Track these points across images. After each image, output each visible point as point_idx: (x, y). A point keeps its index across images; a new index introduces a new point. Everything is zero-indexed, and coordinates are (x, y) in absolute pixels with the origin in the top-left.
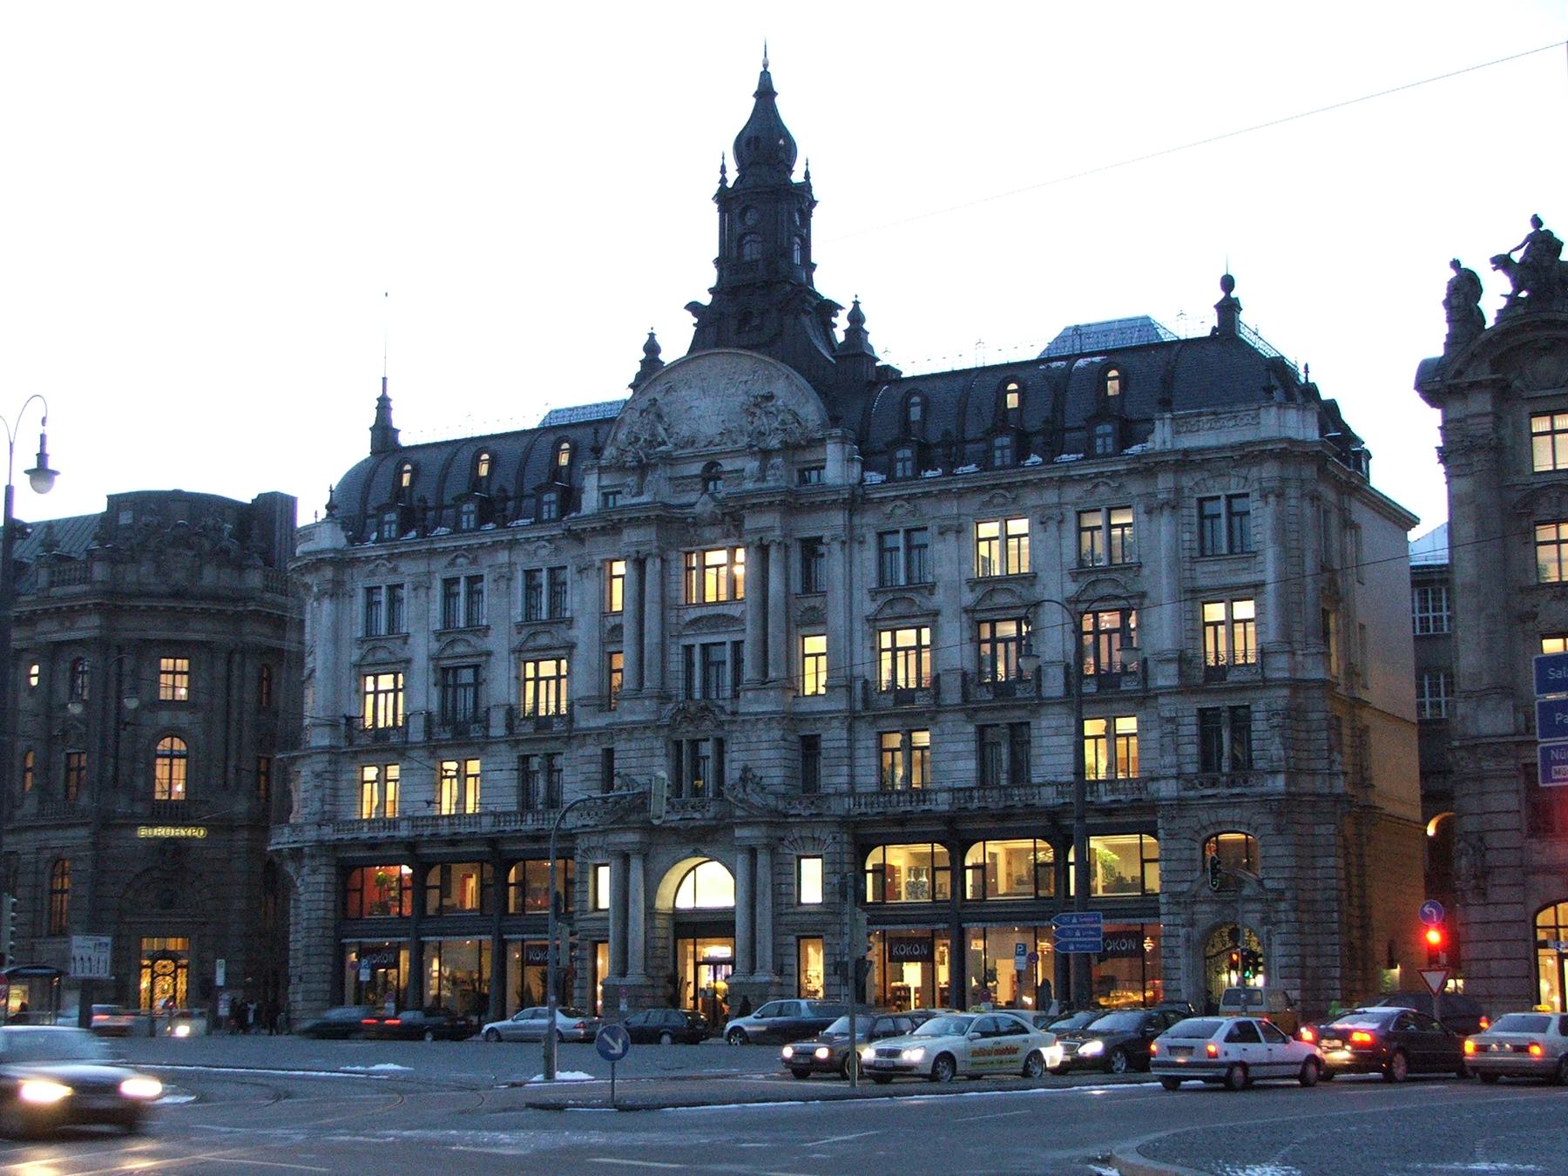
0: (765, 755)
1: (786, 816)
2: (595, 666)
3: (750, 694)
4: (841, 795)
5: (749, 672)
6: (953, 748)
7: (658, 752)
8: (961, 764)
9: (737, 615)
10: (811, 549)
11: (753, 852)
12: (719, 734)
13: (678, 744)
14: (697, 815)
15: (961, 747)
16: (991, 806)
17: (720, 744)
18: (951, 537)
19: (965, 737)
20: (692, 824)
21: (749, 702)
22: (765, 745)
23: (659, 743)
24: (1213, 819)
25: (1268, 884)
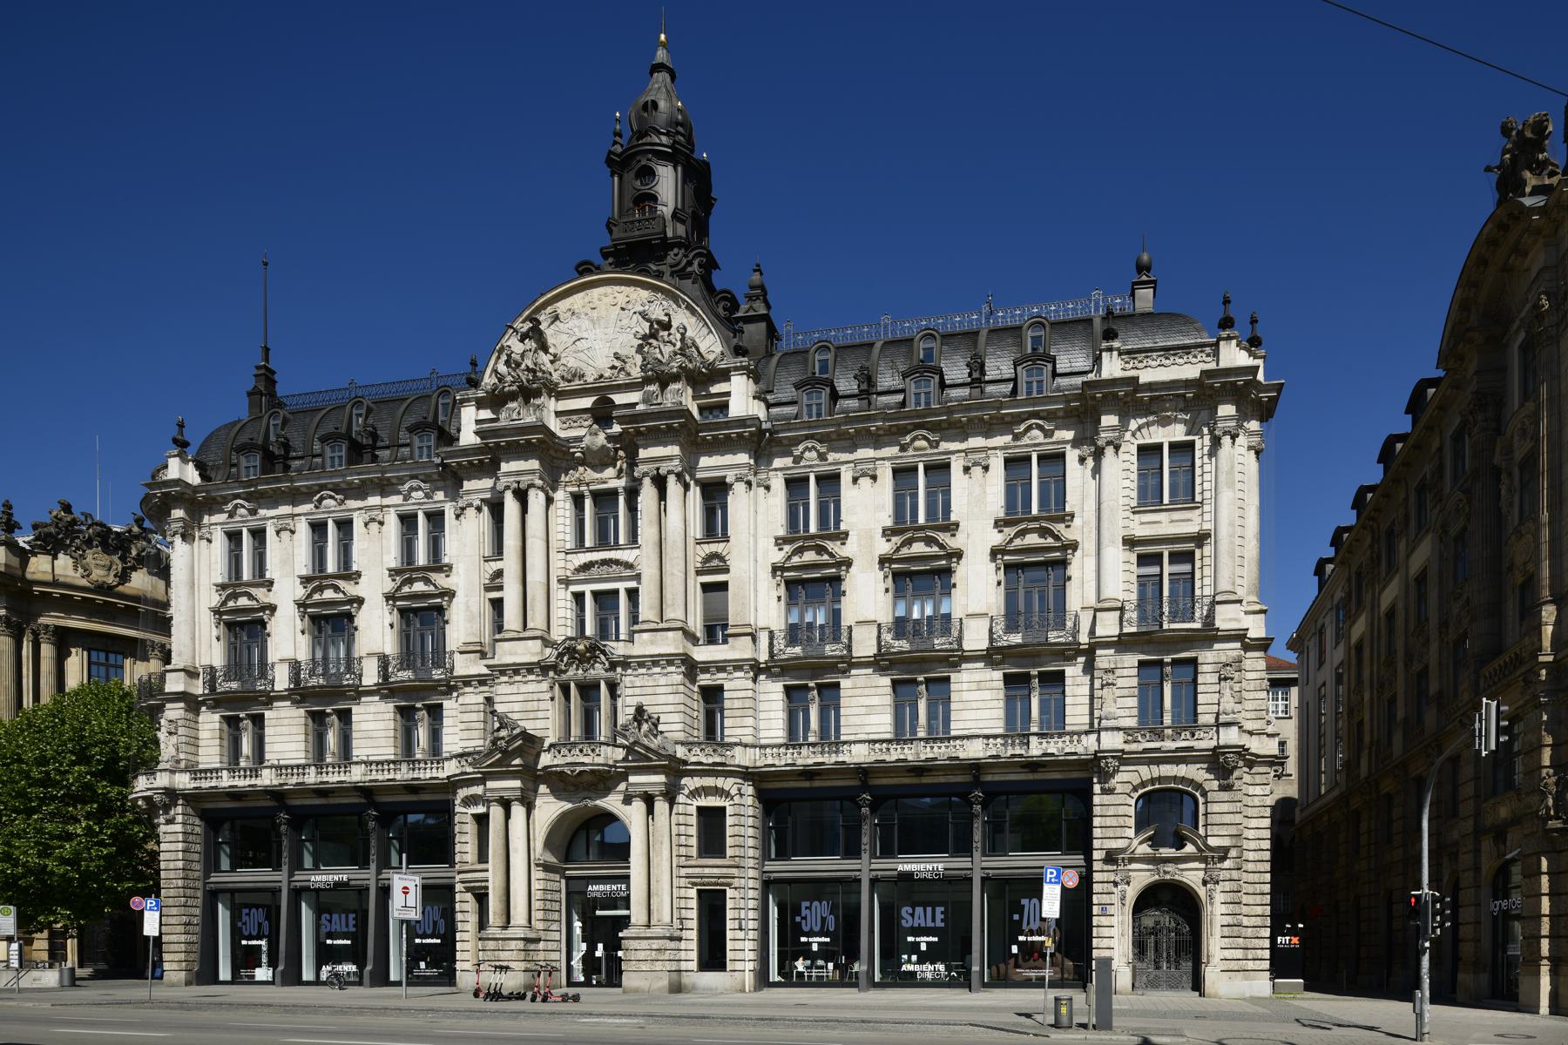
0: (662, 699)
1: (685, 763)
2: (475, 609)
3: (645, 635)
4: (746, 746)
5: (647, 611)
6: (867, 701)
8: (874, 719)
9: (631, 560)
10: (715, 492)
11: (649, 800)
13: (565, 689)
15: (875, 701)
16: (910, 758)
17: (613, 687)
18: (865, 482)
19: (880, 691)
21: (644, 643)
23: (545, 686)
24: (1156, 775)
25: (1212, 842)
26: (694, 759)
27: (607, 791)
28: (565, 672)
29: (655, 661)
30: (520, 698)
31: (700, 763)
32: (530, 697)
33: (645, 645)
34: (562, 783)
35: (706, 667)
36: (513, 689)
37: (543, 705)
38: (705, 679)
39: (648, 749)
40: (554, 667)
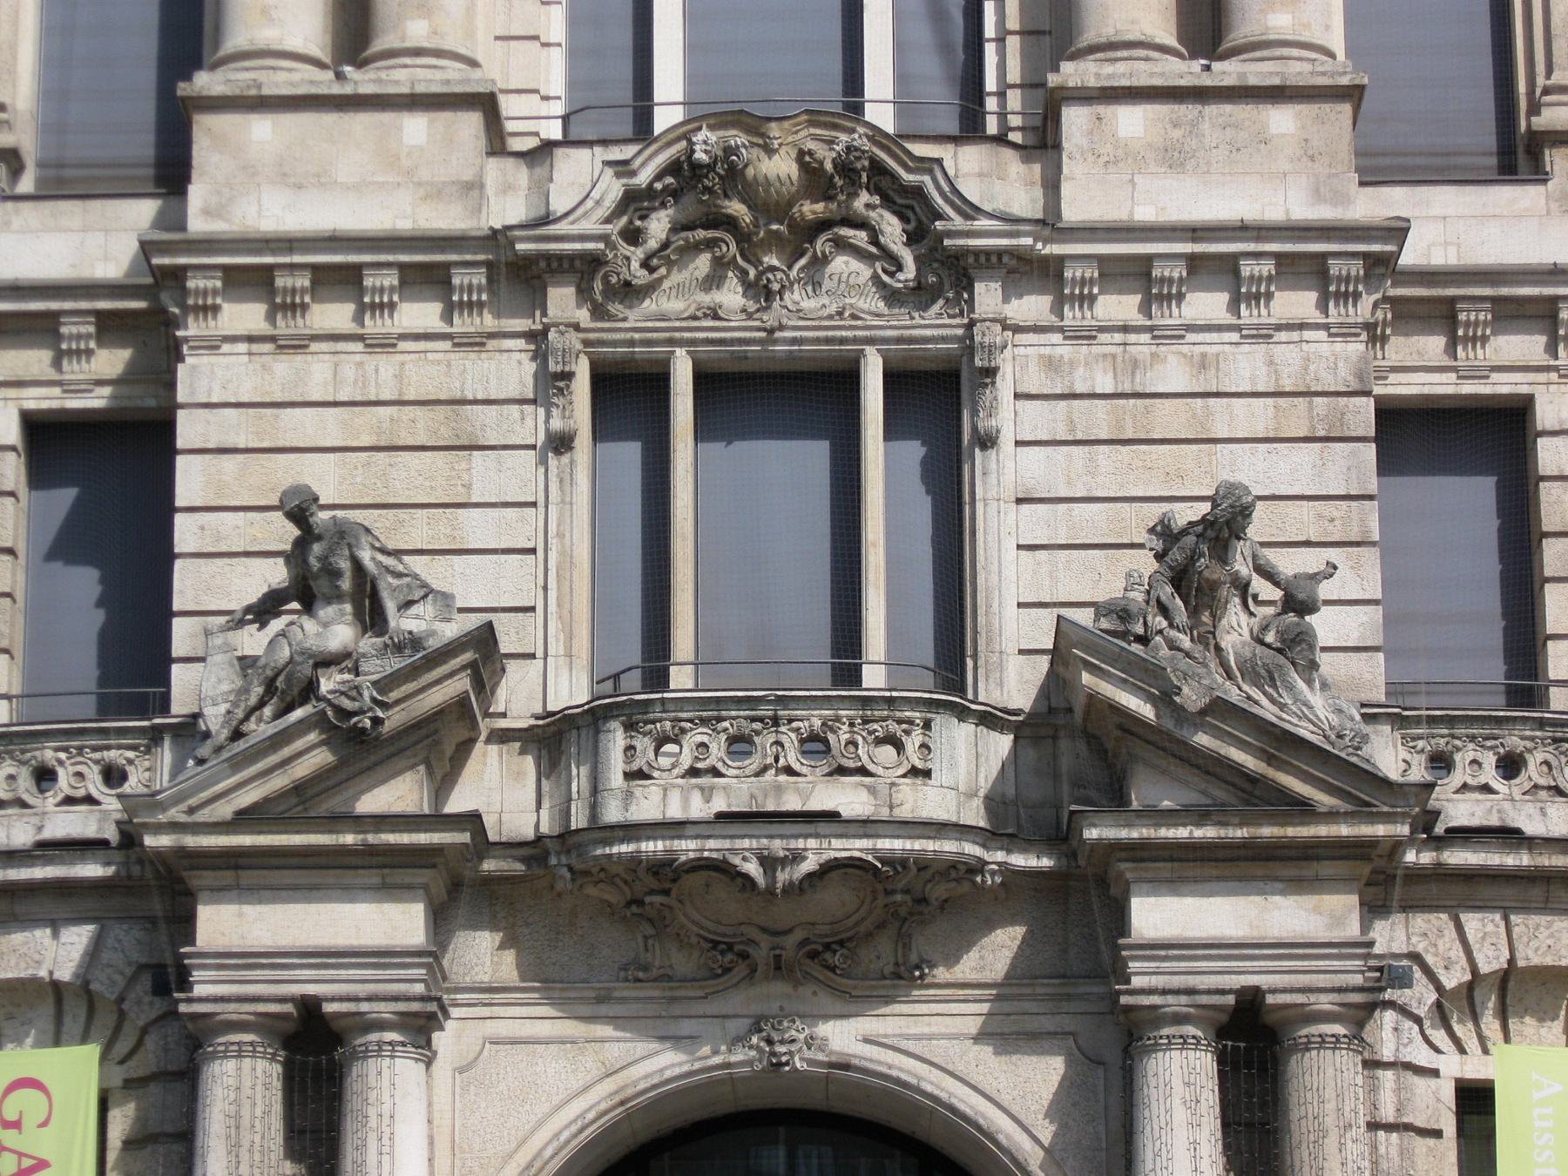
3: (1131, 120)
7: (490, 424)
12: (933, 327)
13: (629, 395)
14: (849, 799)
17: (938, 397)
20: (816, 851)
21: (1122, 159)
22: (1255, 416)
23: (513, 369)
26: (1461, 811)
27: (903, 978)
28: (629, 292)
29: (1215, 257)
30: (365, 426)
31: (1508, 836)
32: (420, 425)
33: (1129, 172)
34: (601, 914)
35: (1438, 304)
36: (281, 376)
37: (490, 476)
38: (1422, 368)
39: (1282, 744)
40: (584, 269)
